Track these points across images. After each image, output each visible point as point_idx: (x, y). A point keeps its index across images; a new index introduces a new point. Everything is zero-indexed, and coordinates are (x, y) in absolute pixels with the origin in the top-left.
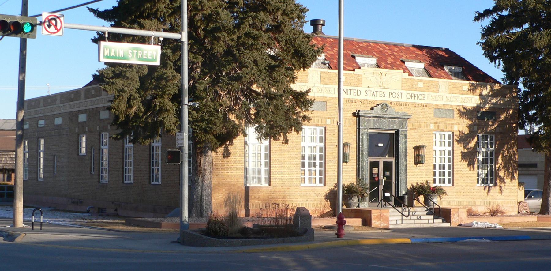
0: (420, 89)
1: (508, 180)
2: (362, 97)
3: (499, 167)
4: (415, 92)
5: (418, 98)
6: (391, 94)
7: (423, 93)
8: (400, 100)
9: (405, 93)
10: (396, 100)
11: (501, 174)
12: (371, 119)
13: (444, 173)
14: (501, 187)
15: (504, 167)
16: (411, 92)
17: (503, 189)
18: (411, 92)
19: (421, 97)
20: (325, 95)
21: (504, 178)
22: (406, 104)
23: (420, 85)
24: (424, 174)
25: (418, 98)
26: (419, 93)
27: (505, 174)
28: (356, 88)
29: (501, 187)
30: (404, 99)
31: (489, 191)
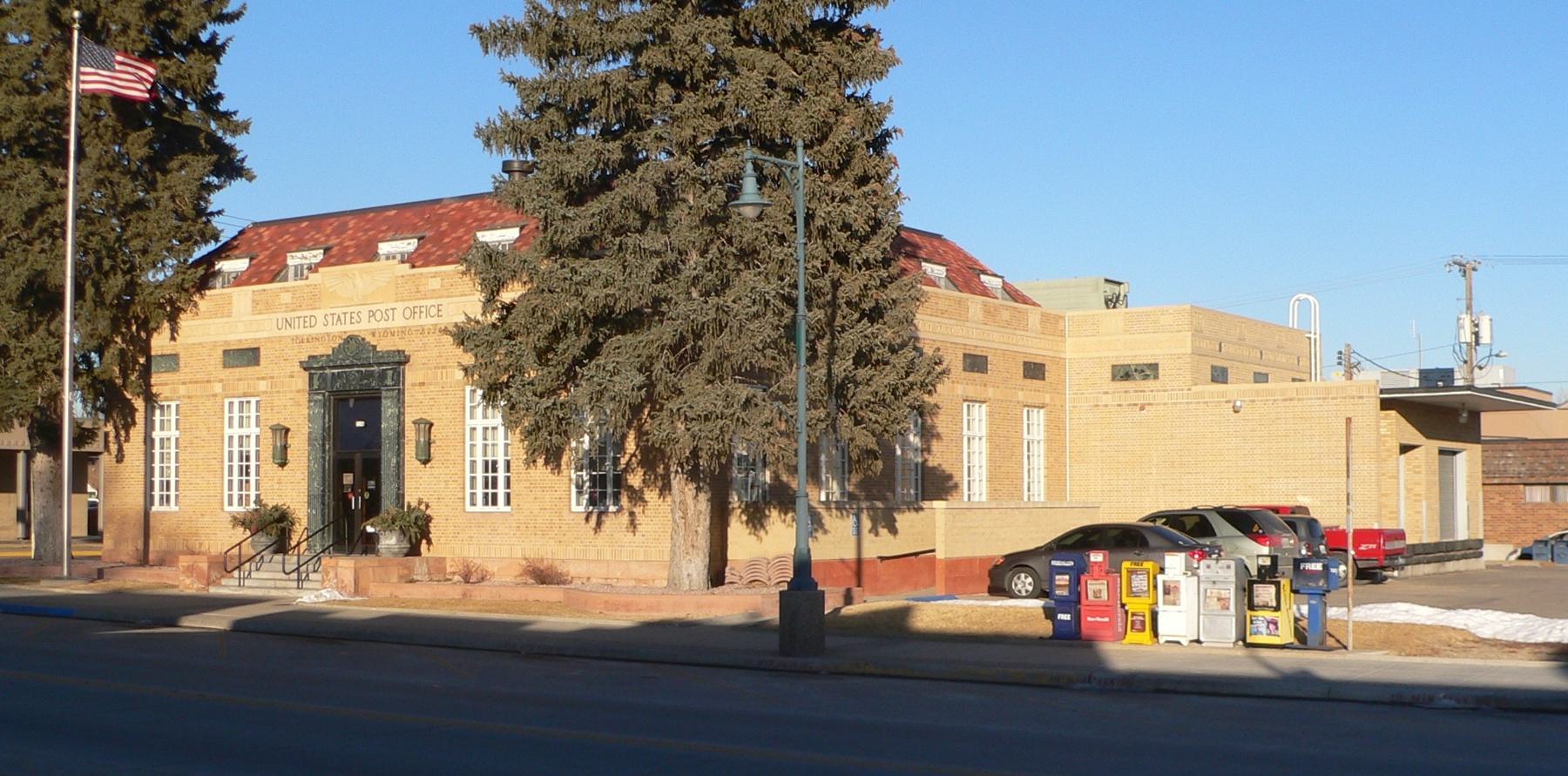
0: (434, 294)
1: (651, 495)
2: (319, 329)
3: (627, 464)
4: (422, 303)
5: (428, 314)
6: (372, 314)
7: (439, 301)
8: (390, 324)
9: (400, 306)
10: (383, 325)
11: (635, 480)
12: (327, 371)
13: (495, 479)
14: (632, 514)
15: (641, 463)
16: (411, 304)
17: (640, 518)
18: (411, 304)
19: (433, 311)
20: (258, 335)
21: (641, 491)
22: (403, 331)
23: (435, 284)
24: (443, 485)
25: (428, 314)
26: (429, 302)
27: (644, 481)
28: (308, 313)
29: (632, 514)
30: (399, 322)
31: (599, 524)
